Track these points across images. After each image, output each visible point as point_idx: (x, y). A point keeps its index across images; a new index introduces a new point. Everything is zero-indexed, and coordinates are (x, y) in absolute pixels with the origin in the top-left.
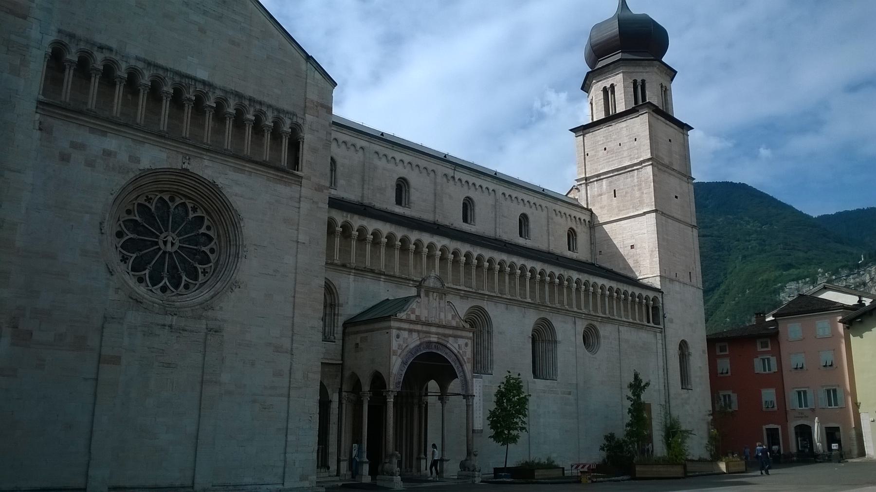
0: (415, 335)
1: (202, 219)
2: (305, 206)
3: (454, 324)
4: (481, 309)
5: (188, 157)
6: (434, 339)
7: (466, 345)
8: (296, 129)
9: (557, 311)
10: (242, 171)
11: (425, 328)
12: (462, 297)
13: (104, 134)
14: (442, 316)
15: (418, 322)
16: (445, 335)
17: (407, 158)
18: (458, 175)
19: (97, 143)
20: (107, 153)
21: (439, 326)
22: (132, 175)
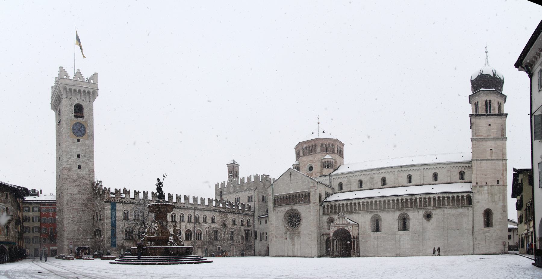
0: (336, 228)
1: (298, 215)
2: (312, 207)
3: (347, 223)
4: (378, 215)
5: (292, 206)
6: (341, 228)
7: (351, 228)
8: (309, 194)
9: (410, 210)
10: (300, 205)
11: (338, 226)
12: (370, 213)
13: (281, 208)
14: (343, 222)
15: (337, 224)
16: (344, 226)
17: (383, 171)
18: (403, 169)
19: (280, 209)
20: (282, 210)
21: (342, 224)
22: (285, 212)
